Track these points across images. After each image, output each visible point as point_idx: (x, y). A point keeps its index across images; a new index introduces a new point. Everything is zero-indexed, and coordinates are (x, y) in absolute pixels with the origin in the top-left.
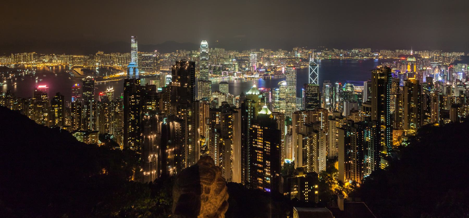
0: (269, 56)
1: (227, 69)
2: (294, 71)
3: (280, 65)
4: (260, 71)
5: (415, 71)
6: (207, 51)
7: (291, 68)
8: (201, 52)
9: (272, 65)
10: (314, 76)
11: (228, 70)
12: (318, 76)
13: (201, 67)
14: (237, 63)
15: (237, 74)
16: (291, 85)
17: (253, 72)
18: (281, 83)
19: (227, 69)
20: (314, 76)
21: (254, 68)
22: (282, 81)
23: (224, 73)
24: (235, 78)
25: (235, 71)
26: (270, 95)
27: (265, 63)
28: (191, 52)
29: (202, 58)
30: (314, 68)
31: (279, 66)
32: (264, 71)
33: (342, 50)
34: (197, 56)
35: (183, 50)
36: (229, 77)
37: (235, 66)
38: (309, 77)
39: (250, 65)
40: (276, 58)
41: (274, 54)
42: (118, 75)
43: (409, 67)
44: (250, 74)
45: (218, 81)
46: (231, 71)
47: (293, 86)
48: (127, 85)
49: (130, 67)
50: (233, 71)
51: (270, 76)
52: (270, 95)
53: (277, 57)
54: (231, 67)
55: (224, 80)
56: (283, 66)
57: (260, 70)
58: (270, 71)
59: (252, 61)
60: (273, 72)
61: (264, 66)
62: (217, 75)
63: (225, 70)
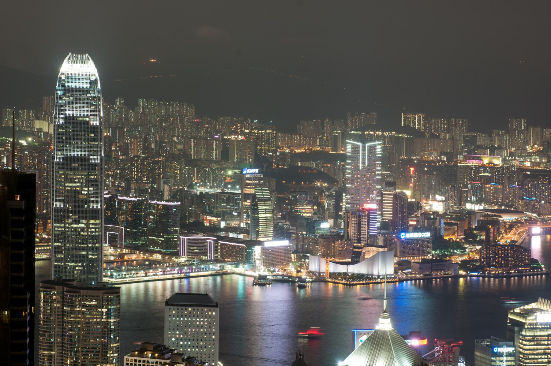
0: (451, 156)
3: (516, 212)
4: (402, 241)
11: (213, 230)
15: (265, 251)
17: (363, 244)
19: (209, 220)
21: (364, 220)
22: (533, 305)
23: (191, 243)
24: (256, 274)
25: (253, 237)
27: (427, 198)
32: (423, 240)
36: (217, 267)
37: (255, 209)
39: (344, 205)
40: (492, 168)
41: (481, 147)
44: (341, 254)
45: (155, 289)
46: (231, 235)
50: (241, 236)
51: (462, 272)
53: (498, 162)
54: (231, 213)
55: (189, 283)
56: (534, 215)
57: (403, 236)
58: (458, 245)
59: (352, 181)
60: (479, 247)
61: (426, 215)
62: (152, 252)
63: (198, 227)
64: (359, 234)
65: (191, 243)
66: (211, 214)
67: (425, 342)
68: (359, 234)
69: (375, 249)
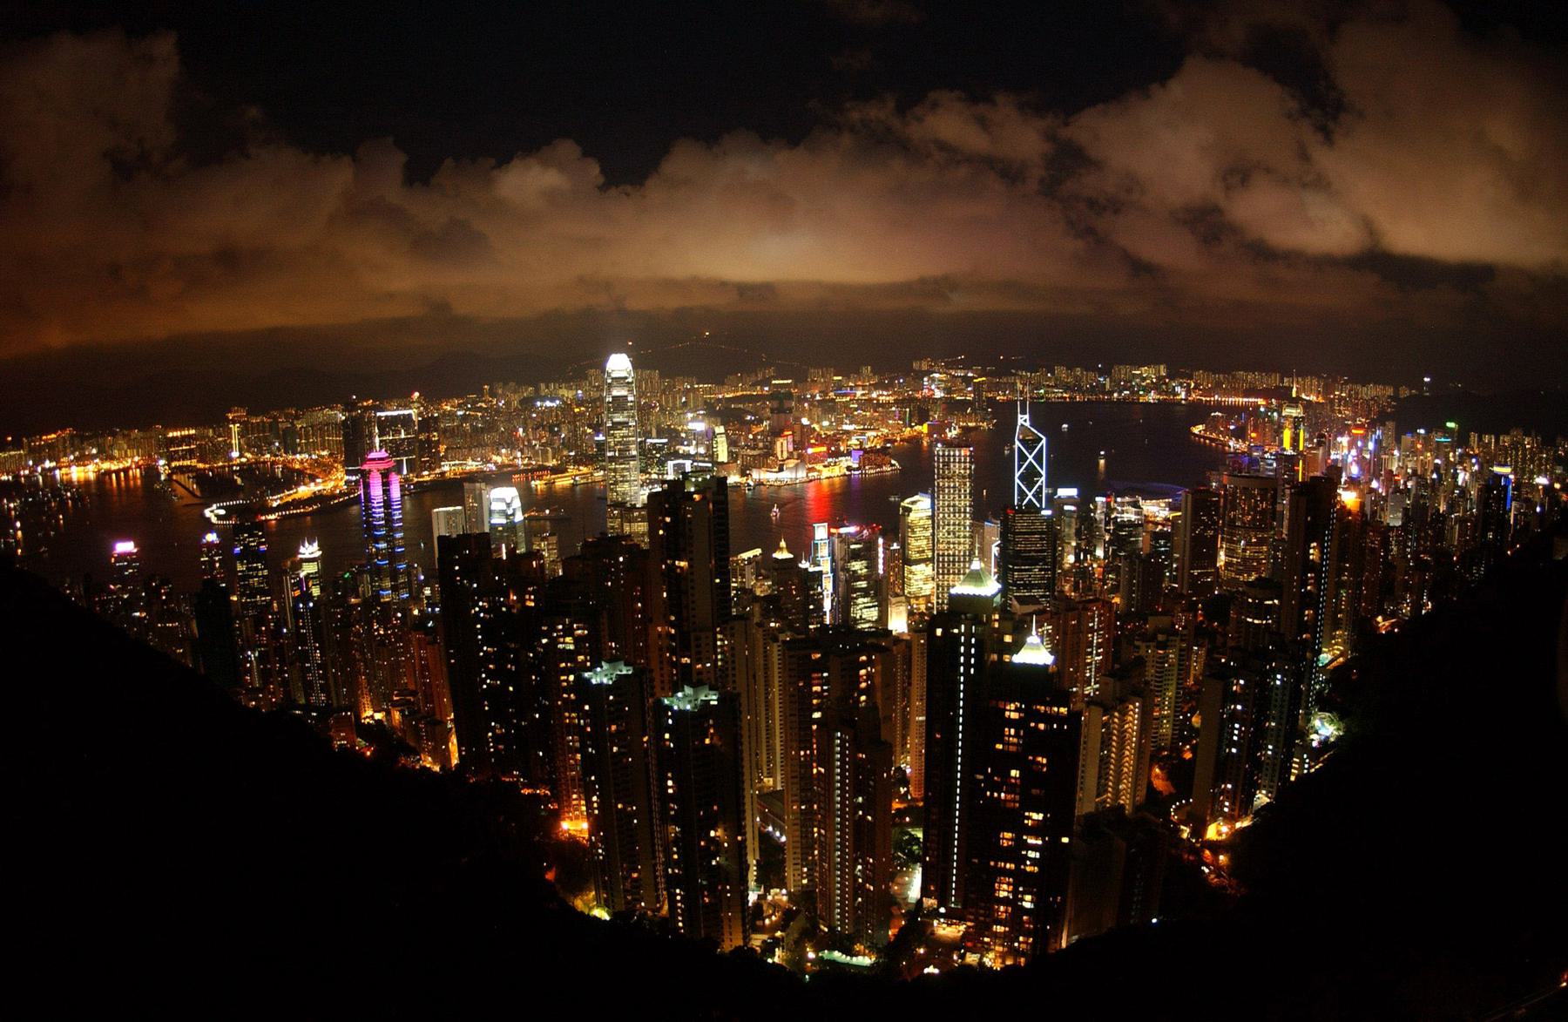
1: (681, 452)
5: (1301, 448)
6: (630, 391)
7: (954, 451)
8: (611, 400)
9: (845, 427)
10: (1030, 477)
11: (687, 456)
16: (954, 513)
18: (913, 503)
19: (682, 449)
22: (916, 498)
26: (881, 550)
28: (537, 390)
29: (615, 420)
30: (1030, 450)
31: (874, 433)
33: (1079, 369)
34: (558, 402)
35: (505, 384)
38: (1017, 481)
42: (304, 491)
43: (1287, 435)
49: (370, 471)
50: (707, 459)
52: (881, 550)
63: (676, 455)
64: (782, 451)
66: (682, 444)
67: (858, 529)
68: (782, 451)
69: (792, 460)
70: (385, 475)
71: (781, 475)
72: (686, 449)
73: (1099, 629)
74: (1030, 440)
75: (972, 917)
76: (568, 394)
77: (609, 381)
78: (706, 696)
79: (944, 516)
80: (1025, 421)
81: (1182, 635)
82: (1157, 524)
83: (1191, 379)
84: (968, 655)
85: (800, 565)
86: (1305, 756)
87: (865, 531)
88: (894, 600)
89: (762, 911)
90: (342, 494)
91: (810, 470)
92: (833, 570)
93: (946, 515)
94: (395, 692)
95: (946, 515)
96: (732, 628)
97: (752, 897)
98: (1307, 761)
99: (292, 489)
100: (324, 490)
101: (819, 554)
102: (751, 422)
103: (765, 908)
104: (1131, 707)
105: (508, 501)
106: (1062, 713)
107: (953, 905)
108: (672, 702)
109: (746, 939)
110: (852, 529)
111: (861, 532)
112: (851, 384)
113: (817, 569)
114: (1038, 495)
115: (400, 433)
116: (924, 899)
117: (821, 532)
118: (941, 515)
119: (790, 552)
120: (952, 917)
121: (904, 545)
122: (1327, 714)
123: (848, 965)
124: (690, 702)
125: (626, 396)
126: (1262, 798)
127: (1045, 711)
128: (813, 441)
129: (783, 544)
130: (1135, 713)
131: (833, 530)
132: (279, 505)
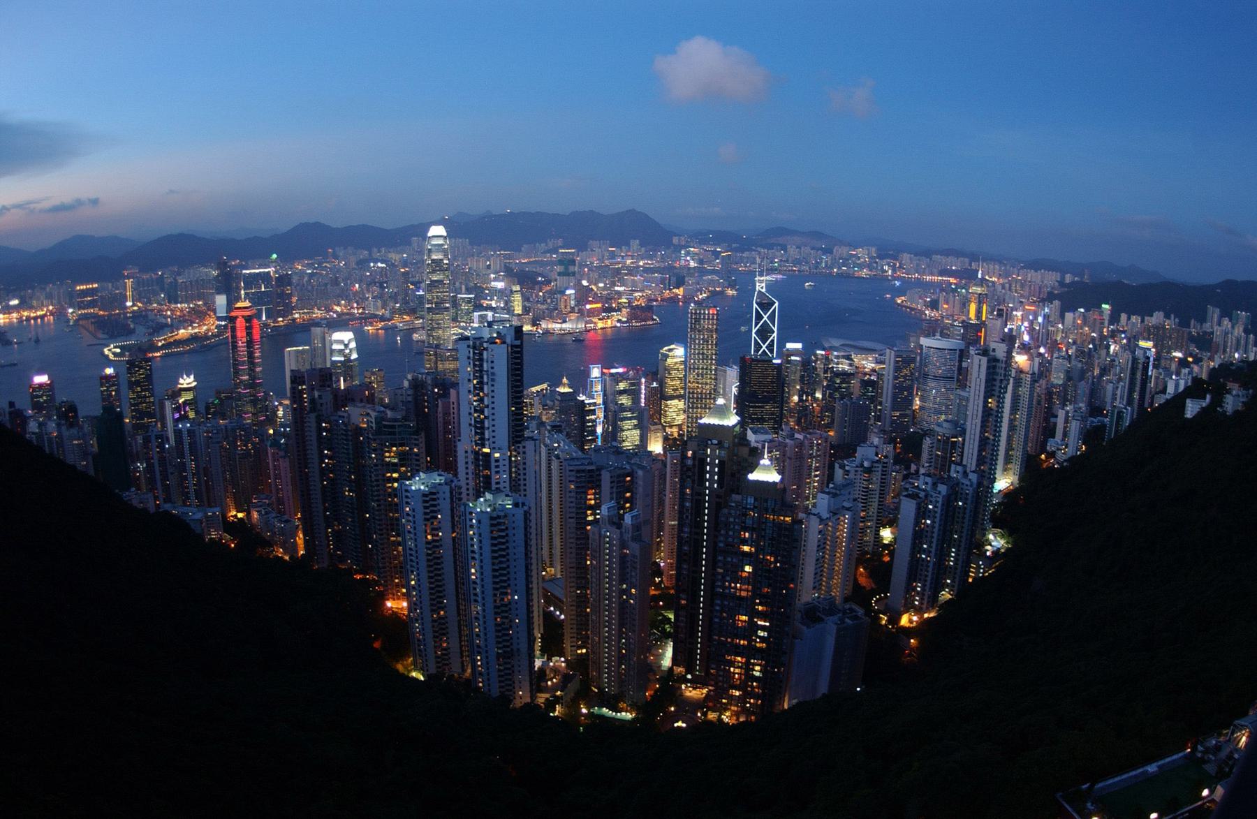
2: (713, 319)
4: (588, 310)
5: (984, 319)
6: (446, 256)
8: (430, 262)
9: (616, 288)
10: (764, 333)
11: (490, 308)
12: (775, 334)
13: (430, 306)
14: (518, 288)
16: (703, 359)
19: (485, 303)
20: (764, 333)
28: (370, 254)
31: (640, 294)
43: (973, 308)
47: (709, 362)
48: (304, 387)
49: (236, 317)
57: (588, 307)
63: (478, 307)
65: (480, 316)
66: (486, 299)
70: (248, 319)
71: (564, 326)
72: (490, 302)
73: (818, 456)
74: (765, 303)
75: (713, 683)
76: (394, 257)
77: (429, 247)
78: (503, 501)
79: (694, 362)
80: (762, 288)
81: (884, 463)
82: (865, 374)
83: (897, 260)
84: (712, 473)
85: (578, 398)
86: (981, 563)
87: (631, 372)
88: (652, 428)
89: (545, 675)
90: (214, 336)
91: (587, 322)
92: (605, 403)
93: (696, 361)
94: (254, 496)
95: (696, 361)
96: (524, 447)
97: (538, 663)
98: (982, 567)
99: (173, 332)
100: (200, 332)
101: (594, 389)
102: (542, 283)
103: (548, 672)
104: (842, 518)
105: (346, 342)
106: (787, 521)
107: (697, 673)
108: (476, 505)
109: (533, 697)
110: (620, 370)
111: (628, 372)
112: (622, 254)
113: (592, 401)
114: (770, 347)
115: (261, 288)
116: (675, 667)
117: (595, 372)
118: (692, 361)
119: (570, 387)
120: (696, 683)
121: (662, 384)
122: (999, 530)
123: (614, 719)
124: (490, 506)
125: (442, 260)
126: (945, 595)
127: (774, 519)
128: (590, 299)
129: (565, 380)
130: (845, 523)
131: (604, 370)
132: (163, 345)
